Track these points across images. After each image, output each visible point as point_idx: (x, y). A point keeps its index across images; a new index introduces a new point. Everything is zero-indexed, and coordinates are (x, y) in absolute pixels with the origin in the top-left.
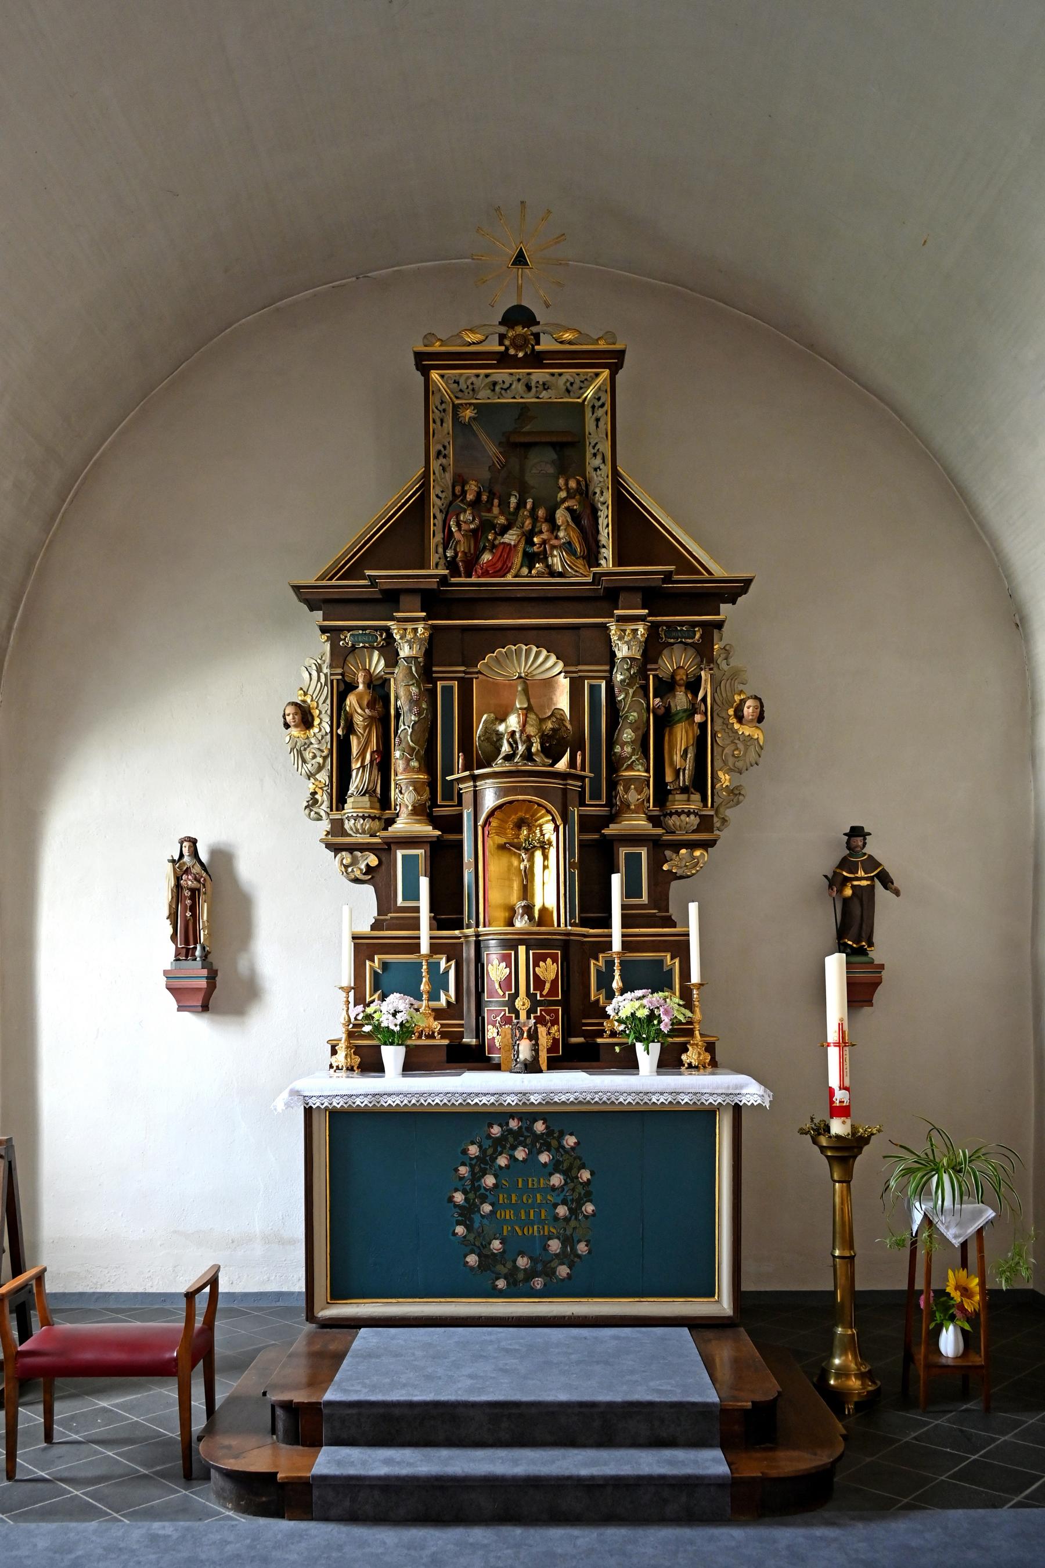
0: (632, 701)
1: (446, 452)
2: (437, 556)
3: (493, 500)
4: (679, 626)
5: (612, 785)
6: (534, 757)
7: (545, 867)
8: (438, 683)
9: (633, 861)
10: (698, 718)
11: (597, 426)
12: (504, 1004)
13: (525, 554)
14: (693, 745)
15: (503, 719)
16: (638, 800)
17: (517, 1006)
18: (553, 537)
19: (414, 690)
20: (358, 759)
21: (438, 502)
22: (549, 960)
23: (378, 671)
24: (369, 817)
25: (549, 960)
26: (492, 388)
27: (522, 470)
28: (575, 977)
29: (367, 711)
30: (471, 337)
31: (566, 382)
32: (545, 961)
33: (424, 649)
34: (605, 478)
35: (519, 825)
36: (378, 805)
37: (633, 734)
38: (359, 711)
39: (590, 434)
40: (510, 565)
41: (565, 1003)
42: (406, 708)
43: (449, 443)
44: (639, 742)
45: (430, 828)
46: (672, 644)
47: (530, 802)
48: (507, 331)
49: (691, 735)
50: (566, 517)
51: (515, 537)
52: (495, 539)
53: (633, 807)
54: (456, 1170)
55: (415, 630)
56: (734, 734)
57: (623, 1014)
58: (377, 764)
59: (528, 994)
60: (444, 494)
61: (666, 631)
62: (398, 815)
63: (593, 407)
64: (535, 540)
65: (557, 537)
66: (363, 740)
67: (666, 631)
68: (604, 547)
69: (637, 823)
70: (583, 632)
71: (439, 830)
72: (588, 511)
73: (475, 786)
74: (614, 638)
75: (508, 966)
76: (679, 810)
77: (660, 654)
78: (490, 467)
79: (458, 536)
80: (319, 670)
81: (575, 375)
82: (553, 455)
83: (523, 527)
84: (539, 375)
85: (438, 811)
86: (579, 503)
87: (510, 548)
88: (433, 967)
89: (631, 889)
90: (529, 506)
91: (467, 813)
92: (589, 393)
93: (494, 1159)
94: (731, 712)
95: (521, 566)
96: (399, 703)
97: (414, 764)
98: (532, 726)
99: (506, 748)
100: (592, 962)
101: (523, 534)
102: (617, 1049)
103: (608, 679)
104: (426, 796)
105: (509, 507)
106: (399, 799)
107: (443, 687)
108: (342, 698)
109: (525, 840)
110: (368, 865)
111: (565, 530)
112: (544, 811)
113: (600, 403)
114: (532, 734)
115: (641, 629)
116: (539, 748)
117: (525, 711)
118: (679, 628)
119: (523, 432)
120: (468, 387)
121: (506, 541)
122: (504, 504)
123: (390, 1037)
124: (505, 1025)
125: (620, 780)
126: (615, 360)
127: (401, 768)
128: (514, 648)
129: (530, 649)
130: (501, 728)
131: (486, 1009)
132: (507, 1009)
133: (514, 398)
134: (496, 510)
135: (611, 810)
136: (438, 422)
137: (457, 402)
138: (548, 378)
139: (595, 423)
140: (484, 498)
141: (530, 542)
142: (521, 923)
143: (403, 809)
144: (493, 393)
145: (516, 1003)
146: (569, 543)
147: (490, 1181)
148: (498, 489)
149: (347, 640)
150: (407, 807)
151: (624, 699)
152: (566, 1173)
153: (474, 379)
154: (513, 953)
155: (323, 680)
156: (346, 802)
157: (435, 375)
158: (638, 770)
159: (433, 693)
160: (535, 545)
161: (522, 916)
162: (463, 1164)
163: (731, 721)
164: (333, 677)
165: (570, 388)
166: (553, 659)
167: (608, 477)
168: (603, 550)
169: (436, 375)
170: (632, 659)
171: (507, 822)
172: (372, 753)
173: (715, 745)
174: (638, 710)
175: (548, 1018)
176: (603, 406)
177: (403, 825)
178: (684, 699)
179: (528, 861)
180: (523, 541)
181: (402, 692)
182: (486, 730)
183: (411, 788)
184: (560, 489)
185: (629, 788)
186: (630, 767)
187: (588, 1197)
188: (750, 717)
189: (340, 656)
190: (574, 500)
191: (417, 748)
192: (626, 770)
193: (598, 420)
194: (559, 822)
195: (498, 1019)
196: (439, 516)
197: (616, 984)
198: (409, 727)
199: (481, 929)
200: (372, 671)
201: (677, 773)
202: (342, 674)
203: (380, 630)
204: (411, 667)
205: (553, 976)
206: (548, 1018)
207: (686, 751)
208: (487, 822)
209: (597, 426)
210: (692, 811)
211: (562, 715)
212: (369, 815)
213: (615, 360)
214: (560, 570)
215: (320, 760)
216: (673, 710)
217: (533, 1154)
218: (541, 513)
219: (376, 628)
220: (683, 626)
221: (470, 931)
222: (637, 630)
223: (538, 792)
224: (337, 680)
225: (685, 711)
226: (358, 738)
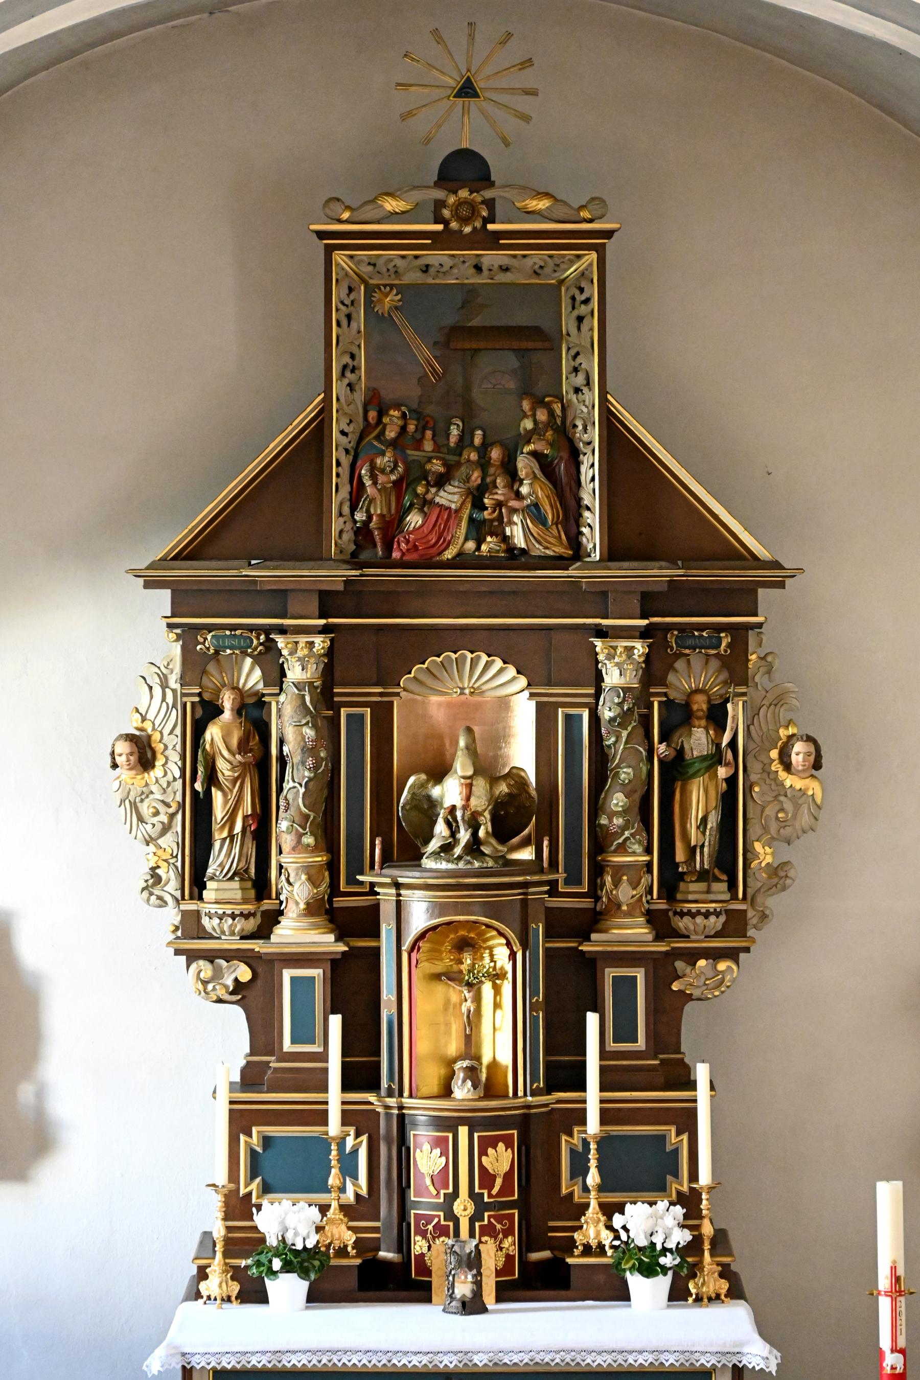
0: (624, 748)
1: (355, 363)
2: (341, 520)
3: (424, 428)
4: (697, 630)
5: (598, 870)
6: (482, 848)
7: (497, 1006)
8: (342, 710)
9: (625, 986)
10: (723, 772)
11: (579, 329)
12: (436, 1207)
13: (471, 520)
14: (716, 807)
16: (633, 897)
17: (456, 1212)
18: (513, 496)
19: (309, 732)
20: (223, 827)
21: (344, 440)
22: (501, 1146)
23: (250, 684)
24: (242, 914)
25: (501, 1146)
26: (424, 269)
27: (468, 387)
28: (539, 1164)
29: (238, 757)
30: (391, 205)
31: (533, 266)
32: (495, 1147)
33: (322, 666)
34: (590, 408)
35: (463, 945)
36: (252, 894)
37: (626, 800)
38: (225, 753)
39: (568, 335)
40: (449, 538)
41: (524, 1204)
42: (297, 759)
43: (359, 346)
44: (637, 809)
45: (331, 938)
46: (689, 655)
47: (475, 922)
48: (447, 196)
49: (712, 793)
50: (531, 468)
51: (456, 498)
52: (427, 491)
53: (624, 908)
55: (311, 644)
56: (779, 788)
58: (252, 832)
59: (472, 1194)
60: (352, 425)
61: (677, 637)
62: (281, 913)
63: (573, 298)
65: (518, 496)
66: (232, 797)
67: (677, 637)
68: (588, 509)
70: (556, 637)
72: (565, 454)
73: (399, 895)
74: (601, 657)
75: (444, 1153)
76: (694, 910)
77: (670, 667)
78: (420, 379)
79: (370, 490)
80: (164, 685)
81: (546, 257)
82: (512, 361)
83: (468, 482)
84: (491, 257)
85: (340, 902)
86: (551, 445)
87: (452, 514)
90: (477, 441)
91: (387, 929)
92: (571, 271)
94: (774, 754)
95: (466, 539)
96: (286, 749)
97: (309, 840)
98: (479, 797)
99: (441, 828)
100: (564, 1138)
101: (469, 492)
103: (594, 706)
104: (324, 886)
105: (448, 439)
106: (284, 891)
107: (349, 716)
109: (469, 971)
110: (236, 980)
111: (531, 484)
112: (494, 933)
113: (583, 297)
114: (480, 809)
116: (490, 829)
117: (469, 781)
118: (696, 633)
119: (471, 329)
120: (388, 270)
121: (442, 502)
124: (438, 1237)
125: (608, 866)
127: (288, 845)
128: (453, 656)
129: (479, 657)
130: (436, 792)
131: (412, 1212)
132: (442, 1214)
133: (457, 279)
134: (428, 446)
135: (596, 902)
136: (344, 322)
138: (506, 261)
139: (576, 324)
140: (411, 428)
141: (479, 505)
142: (462, 1091)
143: (290, 902)
144: (424, 275)
145: (455, 1207)
146: (536, 505)
148: (429, 410)
150: (297, 903)
153: (399, 262)
154: (450, 1135)
156: (205, 887)
157: (339, 257)
158: (634, 853)
159: (334, 722)
160: (486, 508)
161: (464, 1081)
163: (773, 768)
164: (185, 699)
165: (539, 271)
166: (511, 671)
167: (593, 406)
168: (587, 514)
169: (343, 257)
170: (626, 690)
171: (442, 944)
172: (245, 818)
173: (750, 804)
174: (634, 764)
175: (499, 1226)
176: (587, 301)
178: (704, 740)
179: (472, 1002)
180: (469, 505)
181: (290, 734)
182: (413, 795)
183: (304, 877)
184: (525, 416)
185: (620, 880)
186: (622, 849)
188: (800, 768)
190: (544, 442)
191: (312, 815)
192: (615, 851)
193: (580, 319)
194: (517, 947)
195: (430, 1227)
196: (346, 461)
198: (301, 785)
199: (407, 1101)
200: (241, 686)
201: (691, 851)
202: (200, 695)
203: (256, 630)
204: (303, 696)
205: (506, 1167)
206: (499, 1226)
207: (704, 820)
208: (414, 946)
209: (579, 329)
210: (712, 910)
211: (522, 777)
212: (242, 913)
214: (523, 546)
216: (688, 756)
218: (495, 454)
219: (251, 628)
220: (703, 630)
222: (633, 648)
224: (193, 703)
225: (703, 758)
226: (225, 795)
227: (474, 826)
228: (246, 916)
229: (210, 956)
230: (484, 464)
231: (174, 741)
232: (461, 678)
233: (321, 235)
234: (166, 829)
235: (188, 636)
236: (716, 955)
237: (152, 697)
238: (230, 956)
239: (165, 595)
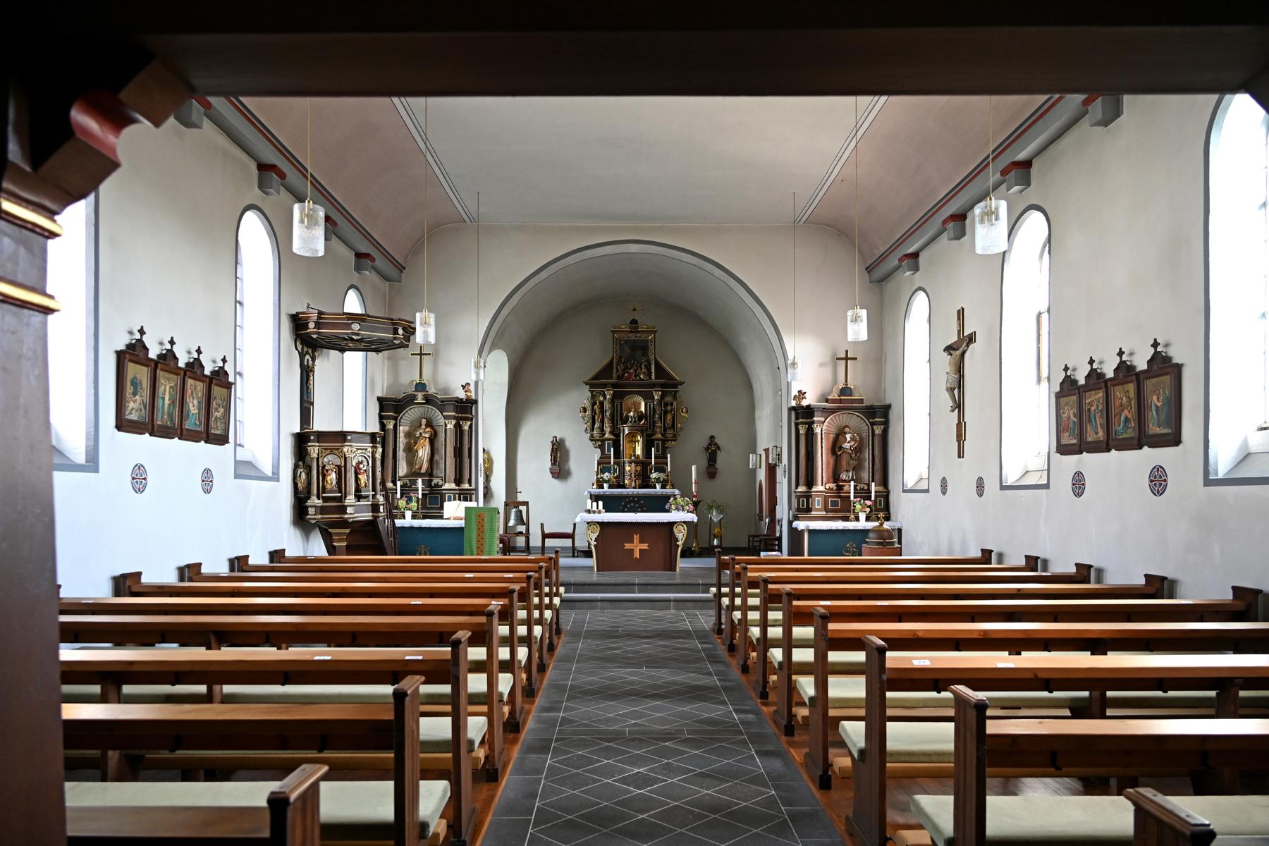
5: (654, 427)
15: (630, 413)
30: (623, 327)
35: (633, 437)
57: (654, 477)
69: (659, 436)
84: (638, 335)
88: (614, 467)
89: (657, 450)
92: (650, 338)
108: (593, 406)
115: (660, 393)
123: (606, 482)
142: (633, 458)
149: (595, 393)
177: (606, 436)
189: (593, 397)
197: (653, 471)
223: (637, 430)
227: (635, 419)
229: (595, 440)
230: (637, 366)
233: (612, 331)
235: (592, 392)
236: (672, 441)
238: (598, 440)
239: (588, 386)
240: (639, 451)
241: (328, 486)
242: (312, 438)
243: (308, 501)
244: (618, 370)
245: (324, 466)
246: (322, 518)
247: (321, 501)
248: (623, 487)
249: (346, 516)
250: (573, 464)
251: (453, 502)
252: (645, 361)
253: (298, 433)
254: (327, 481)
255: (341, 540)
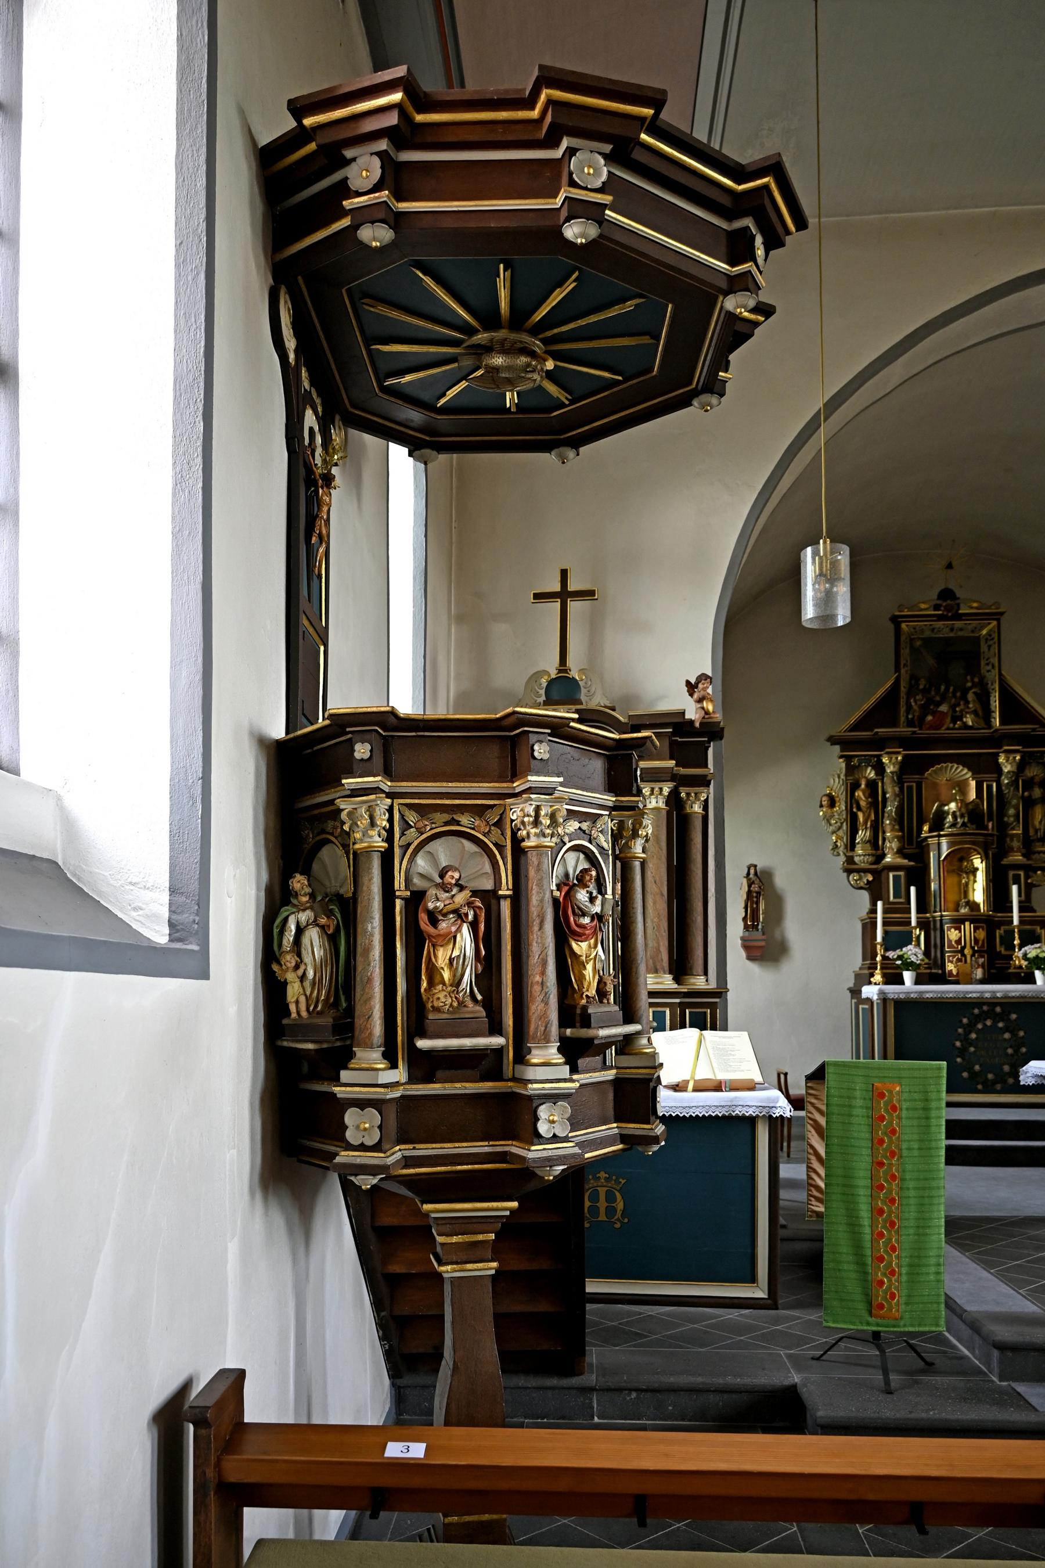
22: (981, 930)
25: (981, 930)
30: (923, 606)
53: (1015, 849)
54: (957, 1031)
63: (987, 639)
64: (957, 709)
65: (968, 708)
66: (867, 814)
68: (993, 712)
69: (1017, 858)
71: (913, 862)
75: (960, 932)
80: (839, 777)
84: (958, 624)
92: (984, 632)
93: (975, 1025)
97: (897, 827)
102: (1023, 975)
121: (942, 710)
122: (938, 689)
123: (908, 965)
126: (997, 616)
137: (912, 637)
147: (973, 1036)
149: (855, 761)
151: (1009, 792)
152: (1011, 1032)
154: (962, 926)
155: (841, 782)
162: (960, 1028)
170: (1013, 772)
172: (872, 821)
176: (993, 639)
186: (1013, 829)
187: (1023, 1045)
189: (850, 770)
195: (955, 959)
209: (989, 649)
213: (997, 616)
215: (839, 824)
217: (995, 1023)
218: (958, 694)
221: (938, 914)
223: (973, 843)
226: (864, 813)
228: (873, 855)
230: (954, 695)
231: (843, 797)
232: (946, 773)
234: (840, 828)
235: (848, 759)
237: (834, 782)
238: (866, 871)
240: (978, 894)
241: (442, 998)
242: (362, 751)
243: (345, 1075)
244: (909, 708)
245: (417, 898)
246: (408, 1162)
247: (399, 1074)
248: (942, 978)
249: (536, 1152)
250: (793, 929)
251: (668, 1034)
252: (974, 685)
253: (279, 744)
254: (433, 972)
255: (471, 1253)
